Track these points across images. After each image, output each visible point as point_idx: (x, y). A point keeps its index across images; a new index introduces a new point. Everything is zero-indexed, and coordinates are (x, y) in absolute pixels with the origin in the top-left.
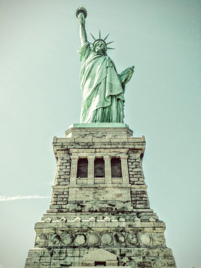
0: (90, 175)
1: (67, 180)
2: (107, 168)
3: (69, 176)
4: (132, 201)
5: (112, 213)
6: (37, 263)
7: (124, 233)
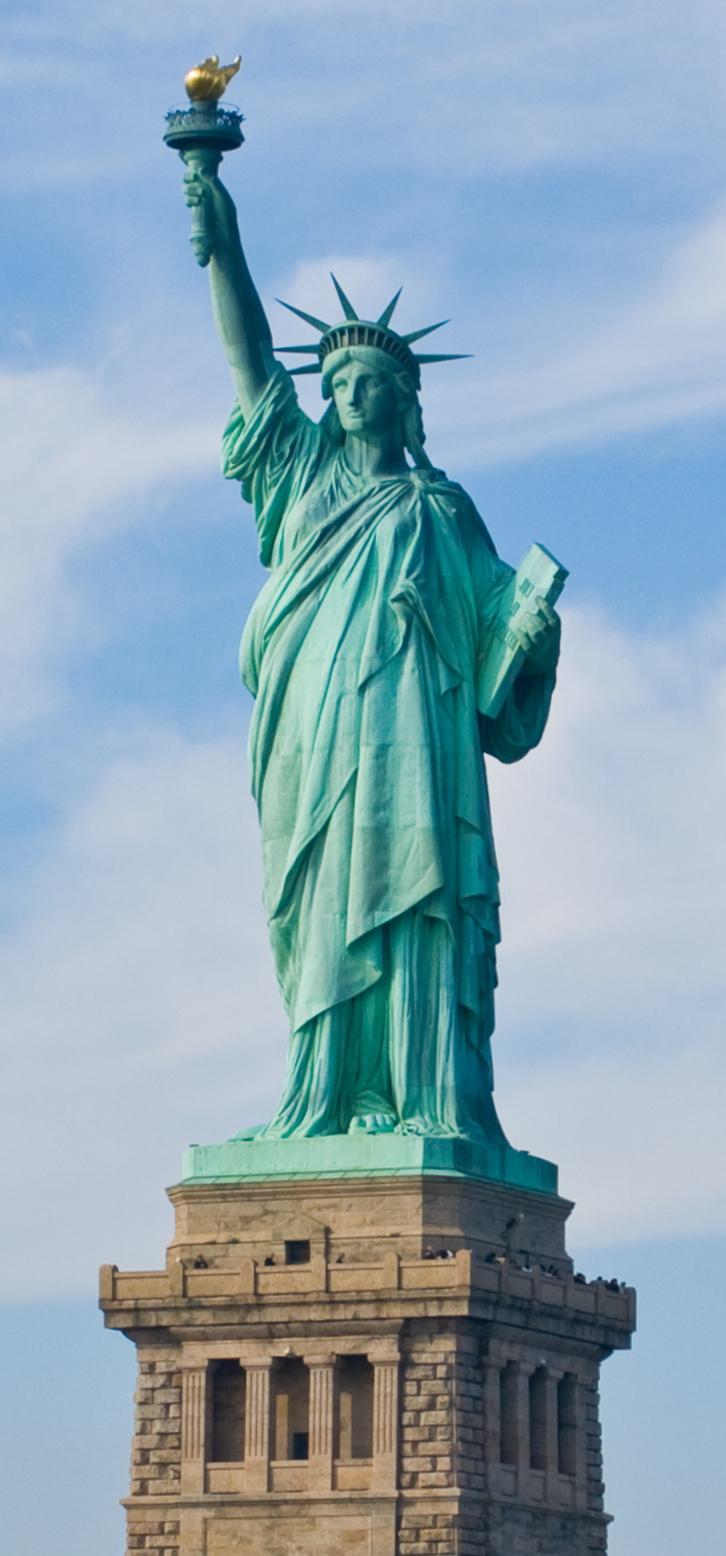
0: (253, 1448)
1: (171, 1473)
2: (317, 1415)
3: (179, 1452)
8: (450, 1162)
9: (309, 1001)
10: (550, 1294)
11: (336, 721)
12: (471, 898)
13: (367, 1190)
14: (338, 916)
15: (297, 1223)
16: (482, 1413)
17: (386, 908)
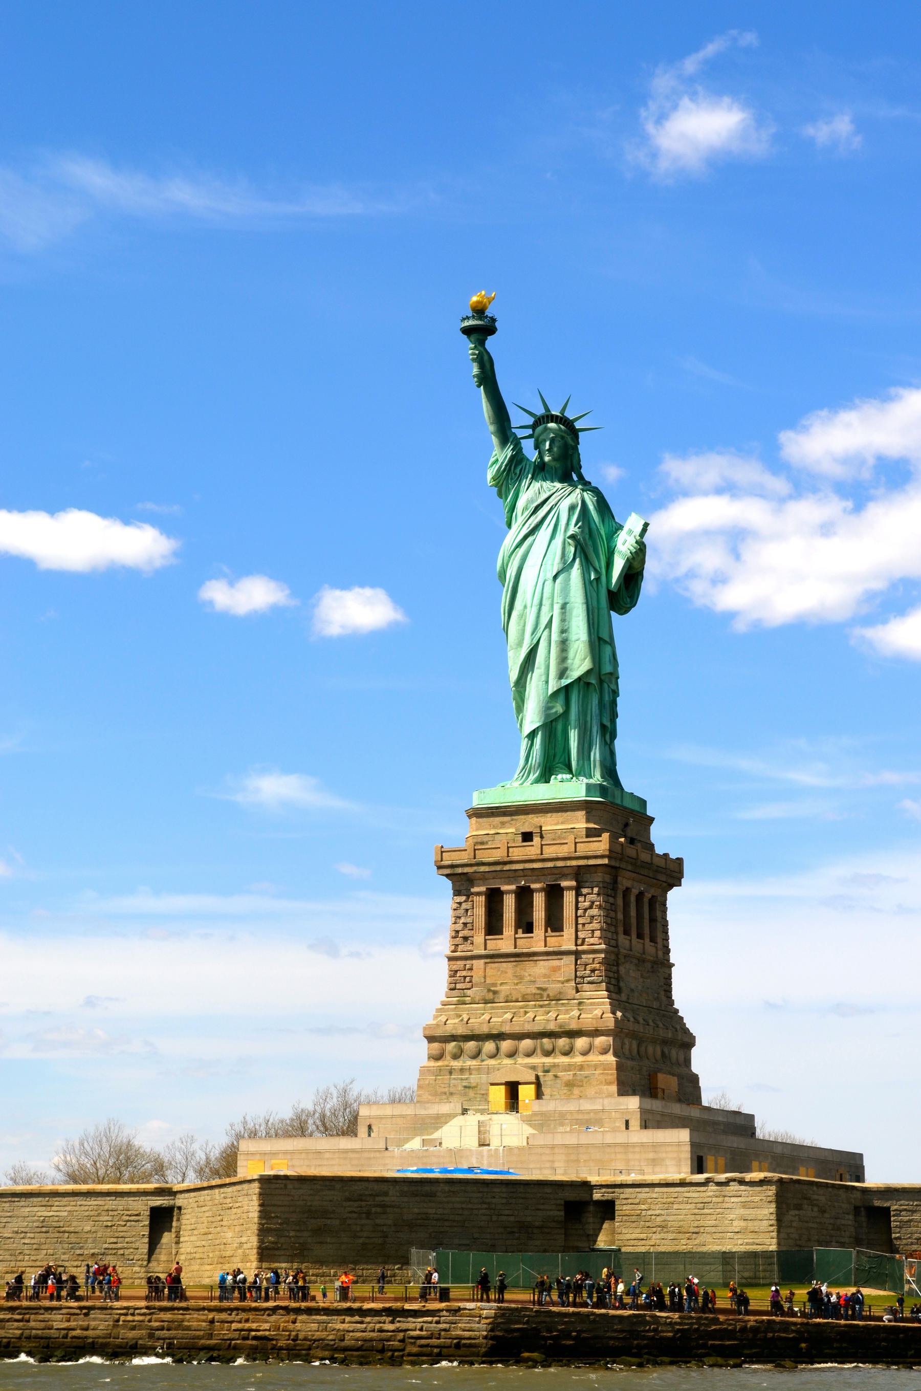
0: (507, 928)
2: (537, 912)
3: (472, 932)
4: (576, 977)
5: (541, 1003)
6: (432, 1084)
7: (553, 1040)
8: (598, 794)
9: (532, 722)
10: (645, 857)
11: (542, 594)
12: (606, 674)
15: (527, 824)
16: (615, 911)
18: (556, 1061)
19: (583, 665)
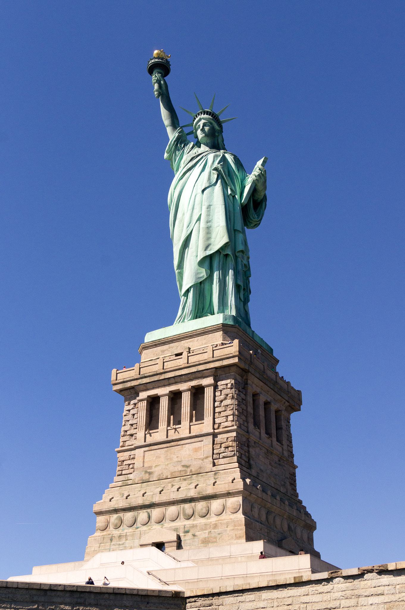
0: (162, 423)
2: (184, 408)
4: (213, 454)
6: (96, 551)
7: (193, 504)
9: (186, 284)
13: (204, 333)
14: (195, 257)
15: (179, 347)
16: (246, 406)
17: (210, 250)
18: (195, 522)
19: (222, 241)
